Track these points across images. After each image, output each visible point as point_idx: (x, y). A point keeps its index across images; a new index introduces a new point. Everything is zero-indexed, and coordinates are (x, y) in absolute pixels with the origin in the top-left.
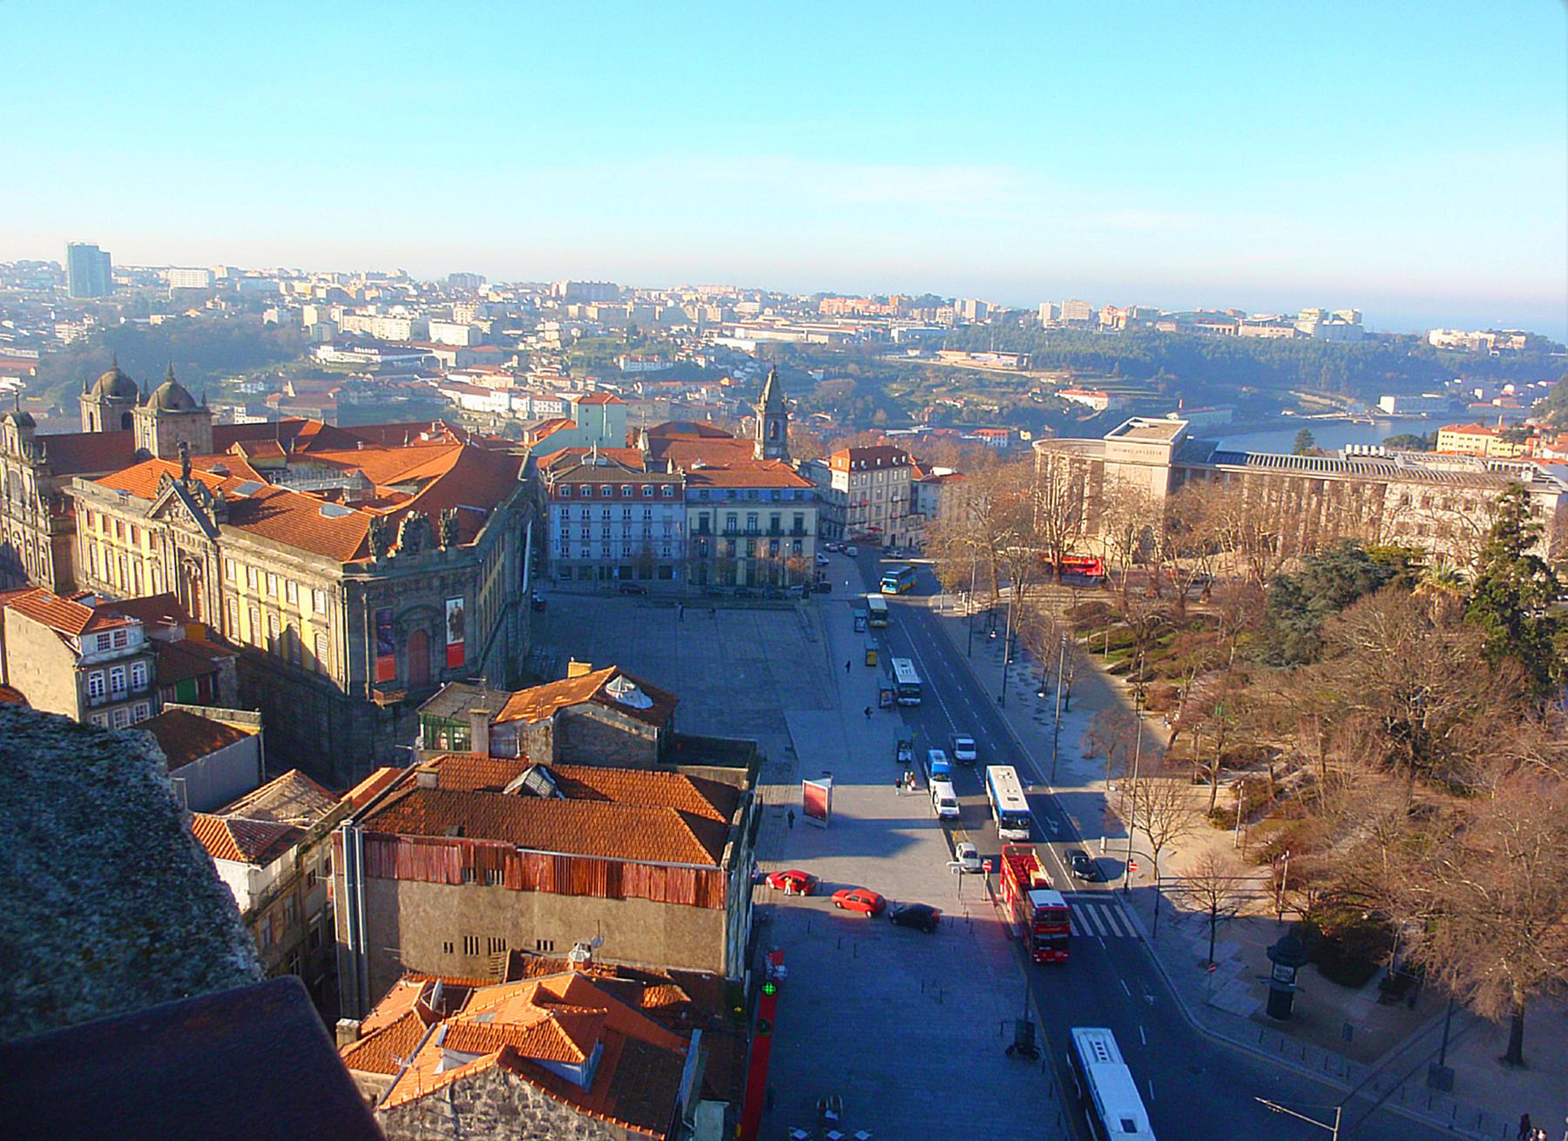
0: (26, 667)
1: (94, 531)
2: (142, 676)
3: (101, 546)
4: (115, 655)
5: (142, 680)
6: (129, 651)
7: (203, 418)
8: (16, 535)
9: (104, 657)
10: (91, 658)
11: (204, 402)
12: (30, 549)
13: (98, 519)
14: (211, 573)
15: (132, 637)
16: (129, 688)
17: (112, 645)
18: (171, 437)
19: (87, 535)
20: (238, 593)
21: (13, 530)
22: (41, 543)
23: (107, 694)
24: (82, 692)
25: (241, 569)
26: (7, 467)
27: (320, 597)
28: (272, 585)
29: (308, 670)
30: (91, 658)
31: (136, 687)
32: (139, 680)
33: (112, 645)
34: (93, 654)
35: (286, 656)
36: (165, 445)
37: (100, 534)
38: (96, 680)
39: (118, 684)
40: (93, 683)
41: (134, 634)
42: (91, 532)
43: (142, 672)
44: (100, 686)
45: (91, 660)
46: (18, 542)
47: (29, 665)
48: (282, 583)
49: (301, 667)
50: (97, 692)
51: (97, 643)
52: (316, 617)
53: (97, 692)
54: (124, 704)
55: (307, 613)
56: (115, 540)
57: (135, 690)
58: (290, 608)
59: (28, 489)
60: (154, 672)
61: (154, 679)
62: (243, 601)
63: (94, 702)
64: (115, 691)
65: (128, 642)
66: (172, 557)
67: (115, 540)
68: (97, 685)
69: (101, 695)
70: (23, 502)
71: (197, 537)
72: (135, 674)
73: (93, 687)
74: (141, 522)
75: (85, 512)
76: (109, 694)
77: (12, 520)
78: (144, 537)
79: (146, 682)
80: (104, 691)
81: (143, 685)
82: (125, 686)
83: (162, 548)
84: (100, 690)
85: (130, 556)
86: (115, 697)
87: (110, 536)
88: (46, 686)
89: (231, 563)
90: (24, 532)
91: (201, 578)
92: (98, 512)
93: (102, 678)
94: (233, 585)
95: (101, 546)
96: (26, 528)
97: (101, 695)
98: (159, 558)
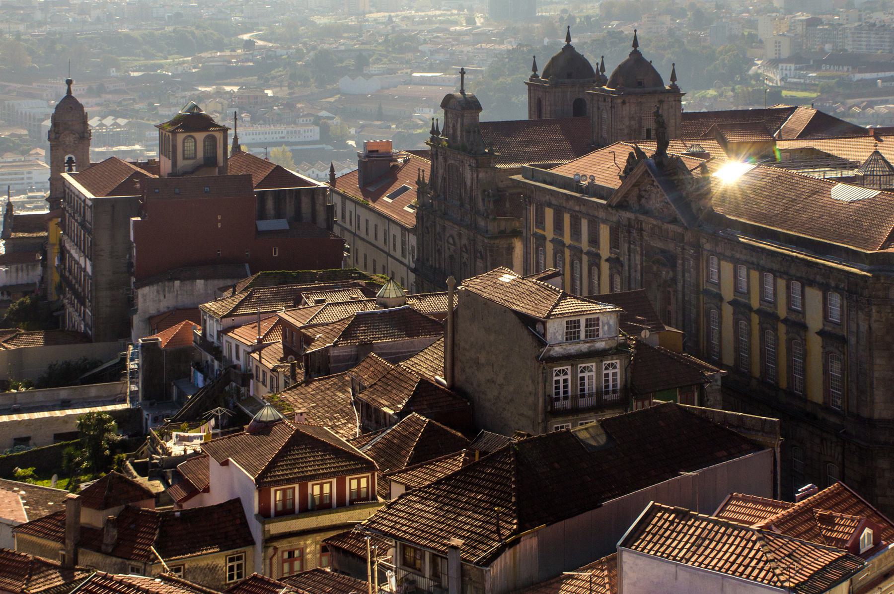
0: (477, 362)
1: (544, 229)
2: (614, 380)
3: (549, 247)
4: (584, 347)
5: (614, 386)
6: (600, 345)
7: (671, 99)
8: (451, 241)
9: (573, 348)
10: (557, 349)
11: (673, 78)
12: (466, 256)
13: (549, 213)
14: (687, 275)
15: (606, 328)
16: (599, 393)
17: (583, 336)
18: (632, 123)
19: (535, 234)
20: (721, 299)
21: (448, 235)
22: (480, 247)
23: (572, 396)
24: (545, 392)
25: (727, 268)
26: (446, 161)
27: (836, 300)
28: (769, 288)
29: (812, 402)
30: (557, 349)
31: (607, 393)
32: (611, 383)
33: (583, 336)
34: (559, 344)
35: (783, 384)
36: (626, 131)
37: (549, 233)
38: (561, 378)
39: (586, 387)
40: (557, 382)
41: (608, 323)
42: (540, 231)
43: (614, 374)
44: (566, 387)
45: (557, 350)
46: (452, 248)
47: (482, 359)
48: (782, 283)
49: (804, 399)
50: (562, 395)
51: (565, 331)
52: (828, 328)
53: (562, 395)
54: (592, 414)
55: (815, 321)
56: (567, 240)
57: (605, 397)
58: (793, 317)
59: (469, 183)
60: (629, 375)
61: (629, 386)
62: (728, 311)
63: (558, 405)
64: (583, 396)
65: (601, 335)
66: (638, 257)
67: (567, 240)
68: (561, 382)
69: (566, 398)
70: (461, 198)
71: (672, 227)
72: (607, 375)
73: (557, 388)
74: (602, 214)
75: (532, 209)
76: (575, 398)
77: (448, 224)
78: (604, 232)
79: (619, 387)
80: (570, 394)
81: (614, 392)
82: (594, 391)
83: (626, 246)
84: (565, 392)
85: (585, 258)
86: (582, 403)
87: (562, 235)
88: (501, 386)
89: (715, 260)
90: (460, 235)
91: (674, 280)
92: (550, 205)
93: (569, 377)
94: (715, 290)
95: (549, 247)
96: (463, 231)
97: (566, 398)
98: (621, 259)
